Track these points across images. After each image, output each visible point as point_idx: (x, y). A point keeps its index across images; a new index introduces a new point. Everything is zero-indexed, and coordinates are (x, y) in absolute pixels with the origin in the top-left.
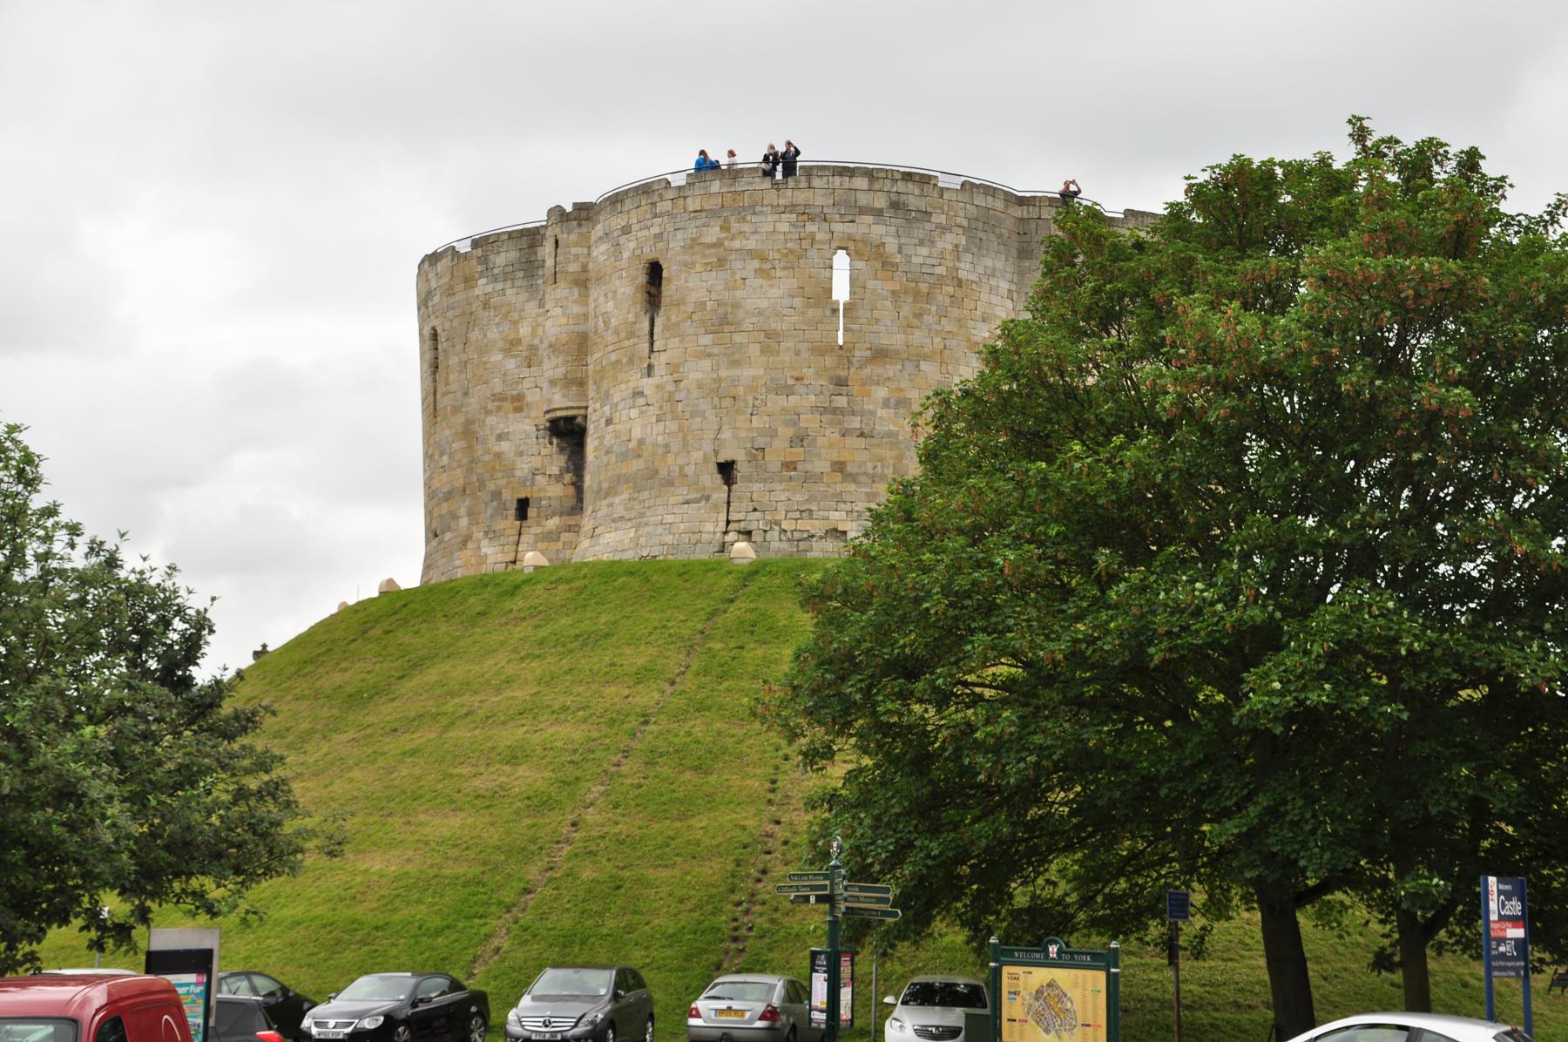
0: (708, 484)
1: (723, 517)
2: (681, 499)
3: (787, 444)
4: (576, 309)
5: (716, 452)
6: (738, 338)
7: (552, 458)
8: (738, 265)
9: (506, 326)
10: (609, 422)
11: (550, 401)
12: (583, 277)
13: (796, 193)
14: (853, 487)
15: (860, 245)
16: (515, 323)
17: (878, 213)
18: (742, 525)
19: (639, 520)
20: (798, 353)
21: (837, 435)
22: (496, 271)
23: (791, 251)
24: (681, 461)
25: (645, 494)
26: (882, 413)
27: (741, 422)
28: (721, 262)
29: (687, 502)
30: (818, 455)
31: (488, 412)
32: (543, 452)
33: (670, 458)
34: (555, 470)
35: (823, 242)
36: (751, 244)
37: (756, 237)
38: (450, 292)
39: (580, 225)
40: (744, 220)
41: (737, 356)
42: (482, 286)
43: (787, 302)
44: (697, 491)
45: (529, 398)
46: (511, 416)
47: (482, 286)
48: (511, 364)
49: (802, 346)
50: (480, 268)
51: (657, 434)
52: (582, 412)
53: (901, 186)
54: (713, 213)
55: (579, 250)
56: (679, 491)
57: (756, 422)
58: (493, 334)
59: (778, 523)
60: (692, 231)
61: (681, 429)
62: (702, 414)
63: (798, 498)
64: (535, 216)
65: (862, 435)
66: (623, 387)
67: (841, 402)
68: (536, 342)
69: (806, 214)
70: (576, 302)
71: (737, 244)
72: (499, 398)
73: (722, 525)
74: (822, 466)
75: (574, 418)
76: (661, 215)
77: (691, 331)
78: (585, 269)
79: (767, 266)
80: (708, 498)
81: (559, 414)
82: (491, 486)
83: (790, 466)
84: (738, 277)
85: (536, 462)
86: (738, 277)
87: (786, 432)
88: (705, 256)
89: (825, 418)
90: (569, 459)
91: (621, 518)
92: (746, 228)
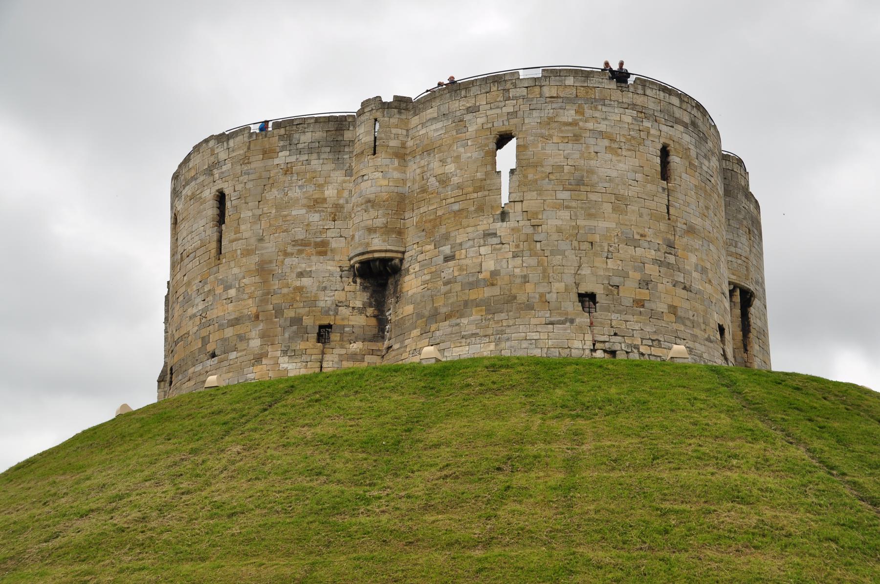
0: (570, 309)
1: (589, 337)
2: (543, 321)
3: (637, 285)
4: (396, 175)
6: (593, 197)
8: (592, 141)
9: (310, 189)
10: (447, 259)
11: (368, 244)
12: (402, 151)
13: (635, 96)
14: (682, 328)
15: (677, 146)
16: (321, 186)
17: (686, 126)
18: (607, 345)
19: (499, 337)
20: (641, 216)
21: (670, 285)
22: (300, 146)
23: (634, 138)
24: (542, 289)
25: (503, 316)
26: (695, 274)
27: (599, 262)
28: (577, 138)
29: (552, 323)
30: (659, 298)
31: (286, 254)
32: (347, 288)
33: (529, 287)
34: (359, 304)
35: (654, 136)
36: (602, 127)
38: (246, 160)
39: (400, 113)
40: (596, 109)
41: (593, 211)
42: (283, 158)
43: (631, 175)
44: (560, 314)
45: (334, 244)
46: (314, 258)
47: (283, 158)
48: (315, 217)
49: (645, 211)
50: (282, 143)
51: (515, 267)
52: (400, 255)
53: (695, 112)
54: (569, 100)
55: (399, 131)
56: (541, 313)
58: (295, 193)
59: (637, 347)
60: (548, 111)
61: (539, 263)
62: (563, 253)
63: (648, 329)
65: (685, 288)
66: (470, 230)
67: (671, 259)
68: (341, 201)
69: (643, 113)
70: (395, 169)
71: (590, 125)
72: (302, 244)
73: (589, 345)
74: (662, 307)
75: (392, 259)
76: (516, 98)
77: (550, 187)
78: (403, 146)
79: (615, 146)
80: (572, 321)
81: (376, 255)
82: (290, 314)
83: (640, 303)
84: (592, 150)
85: (340, 296)
86: (592, 150)
87: (635, 276)
88: (562, 132)
89: (663, 269)
90: (371, 296)
92: (597, 114)
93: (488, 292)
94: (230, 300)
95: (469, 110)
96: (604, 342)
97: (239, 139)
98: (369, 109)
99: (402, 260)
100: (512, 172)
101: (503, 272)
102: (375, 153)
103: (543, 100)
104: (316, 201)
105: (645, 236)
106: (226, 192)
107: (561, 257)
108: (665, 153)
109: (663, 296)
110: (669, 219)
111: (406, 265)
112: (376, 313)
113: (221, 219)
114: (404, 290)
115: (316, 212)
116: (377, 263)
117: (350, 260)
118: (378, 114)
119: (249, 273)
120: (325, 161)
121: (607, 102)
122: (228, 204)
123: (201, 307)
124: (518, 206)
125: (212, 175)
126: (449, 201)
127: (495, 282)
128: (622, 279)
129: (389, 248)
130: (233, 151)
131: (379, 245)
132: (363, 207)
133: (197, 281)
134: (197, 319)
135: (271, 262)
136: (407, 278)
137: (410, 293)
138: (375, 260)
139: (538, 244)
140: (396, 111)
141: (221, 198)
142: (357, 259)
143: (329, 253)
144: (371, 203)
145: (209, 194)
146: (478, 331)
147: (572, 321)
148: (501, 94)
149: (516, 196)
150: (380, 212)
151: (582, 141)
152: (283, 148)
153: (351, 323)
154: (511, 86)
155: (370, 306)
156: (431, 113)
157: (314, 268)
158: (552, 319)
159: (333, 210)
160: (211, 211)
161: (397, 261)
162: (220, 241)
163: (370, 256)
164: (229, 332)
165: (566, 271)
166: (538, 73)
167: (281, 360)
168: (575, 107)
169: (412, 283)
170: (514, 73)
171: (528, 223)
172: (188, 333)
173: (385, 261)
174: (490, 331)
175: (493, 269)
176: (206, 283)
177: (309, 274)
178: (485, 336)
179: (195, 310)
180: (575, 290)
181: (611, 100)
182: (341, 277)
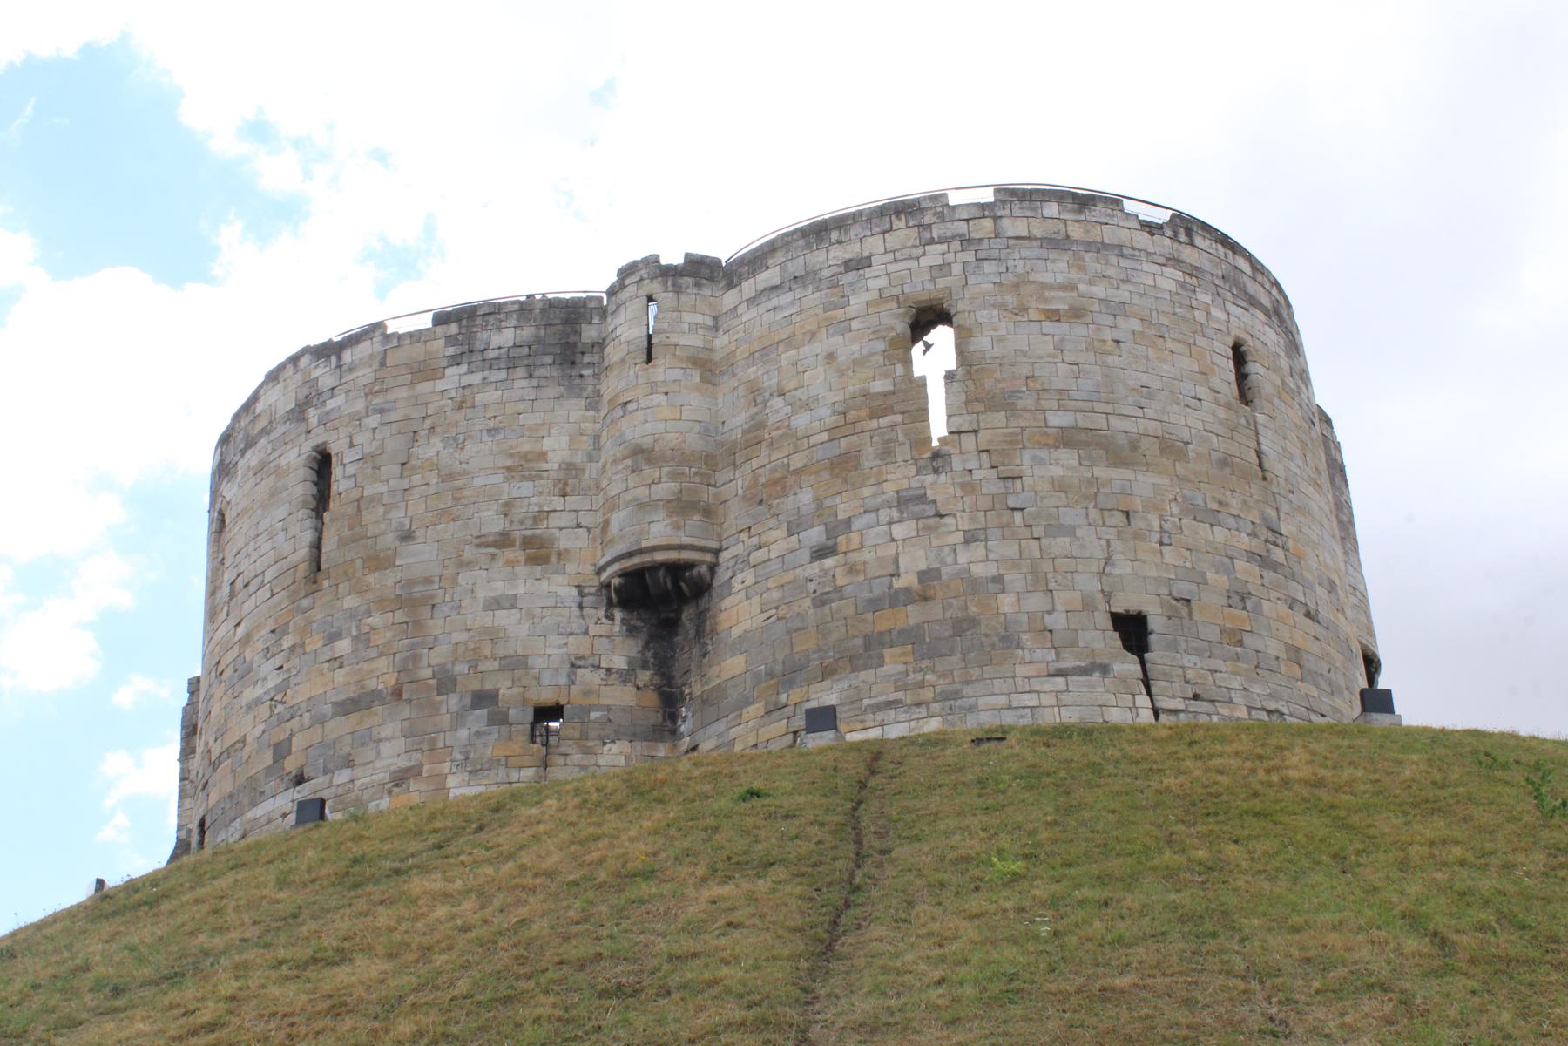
0: (1099, 645)
3: (1224, 601)
5: (1108, 596)
7: (614, 644)
8: (1109, 320)
22: (491, 354)
24: (1036, 602)
31: (463, 564)
32: (593, 630)
33: (1007, 603)
34: (620, 662)
37: (1129, 287)
39: (698, 285)
45: (564, 542)
46: (521, 569)
52: (708, 558)
57: (1169, 555)
62: (1070, 531)
63: (1256, 689)
64: (590, 278)
65: (1308, 614)
68: (579, 459)
71: (1099, 291)
75: (690, 565)
80: (1105, 669)
81: (660, 557)
84: (1108, 335)
85: (578, 645)
90: (646, 647)
91: (890, 704)
93: (913, 615)
94: (338, 662)
95: (850, 265)
96: (1176, 712)
97: (364, 348)
98: (635, 278)
99: (713, 568)
100: (950, 377)
101: (945, 571)
102: (649, 359)
103: (1001, 243)
104: (525, 457)
105: (1227, 505)
106: (333, 449)
107: (1067, 540)
108: (1239, 356)
109: (1274, 625)
110: (1264, 478)
111: (722, 575)
112: (657, 680)
113: (322, 499)
114: (720, 628)
115: (524, 478)
116: (661, 573)
117: (598, 573)
118: (655, 287)
119: (382, 603)
120: (543, 382)
121: (1125, 251)
122: (337, 471)
123: (274, 680)
124: (968, 442)
125: (304, 420)
126: (813, 440)
127: (930, 593)
128: (1194, 587)
129: (686, 540)
130: (351, 370)
131: (661, 534)
132: (629, 462)
133: (265, 632)
134: (264, 711)
135: (428, 581)
136: (726, 603)
137: (736, 632)
138: (654, 568)
139: (1018, 516)
140: (690, 280)
141: (322, 463)
142: (616, 567)
143: (553, 559)
144: (642, 455)
145: (296, 457)
146: (900, 695)
147: (1105, 669)
148: (914, 232)
149: (965, 422)
150: (665, 470)
151: (1088, 319)
152: (456, 361)
153: (604, 702)
154: (934, 219)
155: (645, 666)
156: (769, 277)
157: (521, 590)
158: (1063, 665)
159: (561, 475)
160: (300, 486)
161: (704, 569)
162: (317, 546)
163: (646, 558)
164: (339, 727)
165: (1080, 568)
166: (987, 196)
167: (451, 782)
168: (1067, 256)
169: (739, 611)
170: (938, 199)
171: (993, 473)
172: (243, 741)
173: (677, 570)
174: (928, 694)
175: (923, 567)
176: (285, 633)
177: (512, 603)
178: (918, 705)
179: (259, 691)
180: (1102, 606)
181: (1133, 248)
182: (581, 607)
